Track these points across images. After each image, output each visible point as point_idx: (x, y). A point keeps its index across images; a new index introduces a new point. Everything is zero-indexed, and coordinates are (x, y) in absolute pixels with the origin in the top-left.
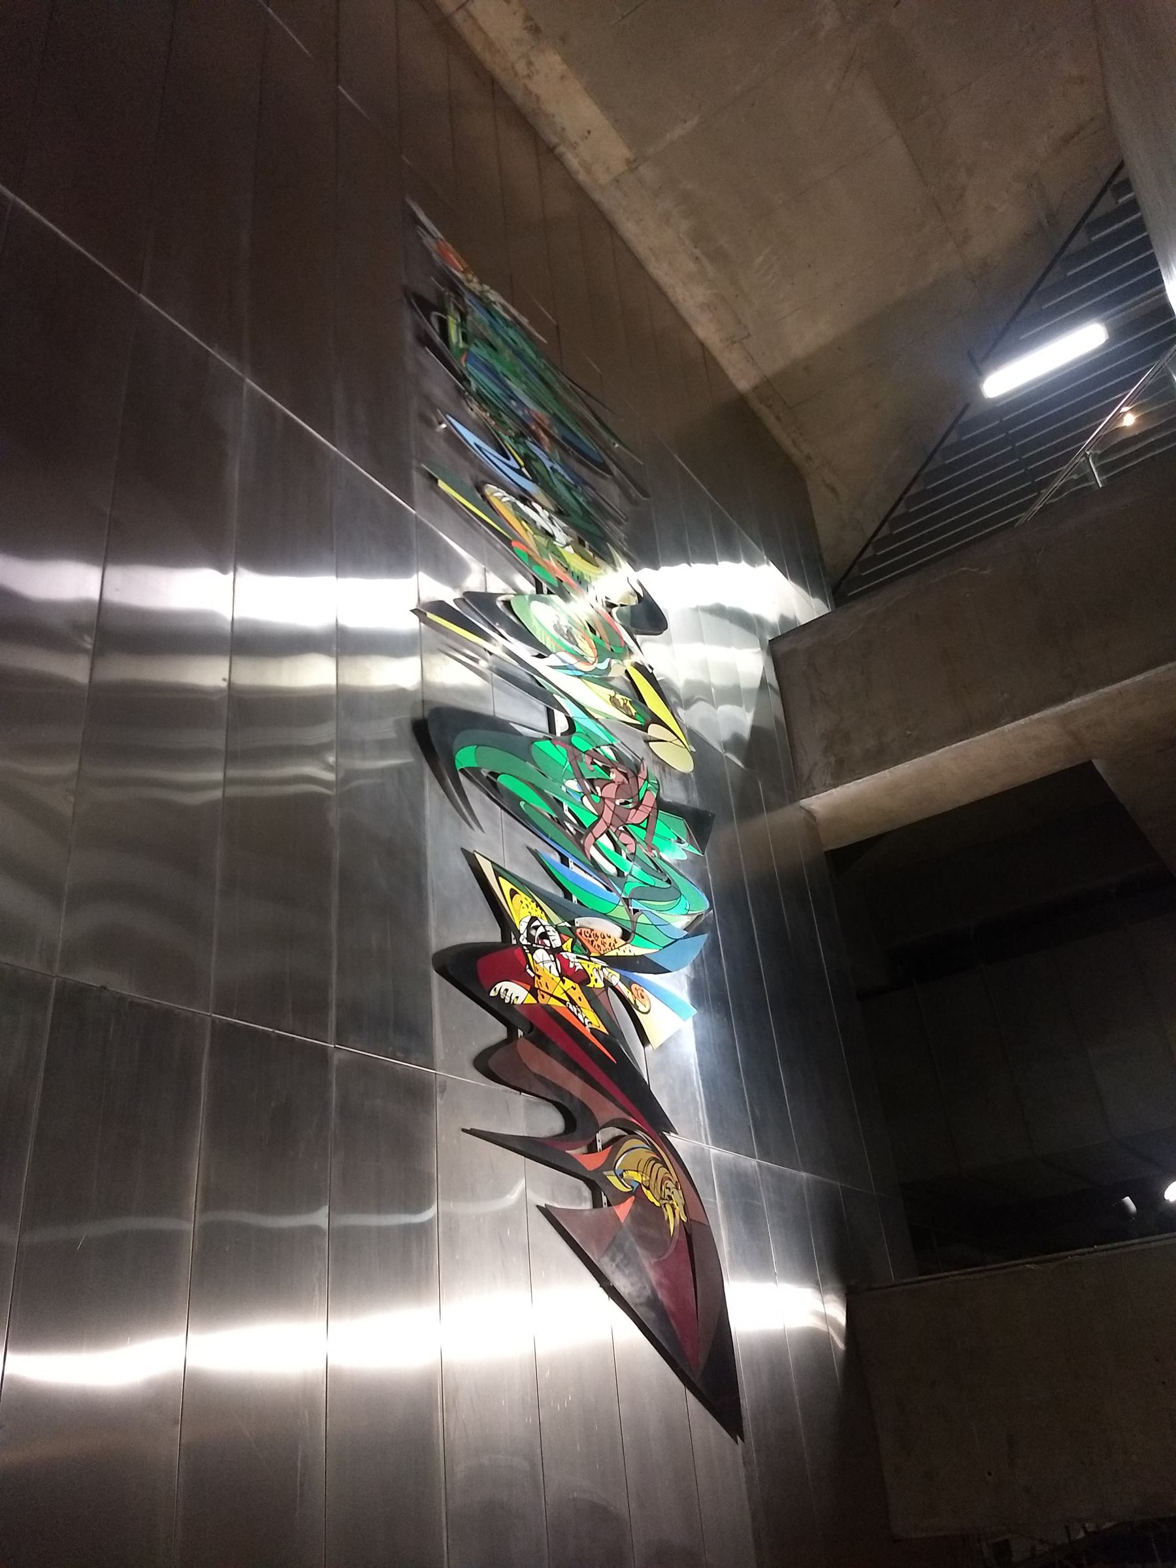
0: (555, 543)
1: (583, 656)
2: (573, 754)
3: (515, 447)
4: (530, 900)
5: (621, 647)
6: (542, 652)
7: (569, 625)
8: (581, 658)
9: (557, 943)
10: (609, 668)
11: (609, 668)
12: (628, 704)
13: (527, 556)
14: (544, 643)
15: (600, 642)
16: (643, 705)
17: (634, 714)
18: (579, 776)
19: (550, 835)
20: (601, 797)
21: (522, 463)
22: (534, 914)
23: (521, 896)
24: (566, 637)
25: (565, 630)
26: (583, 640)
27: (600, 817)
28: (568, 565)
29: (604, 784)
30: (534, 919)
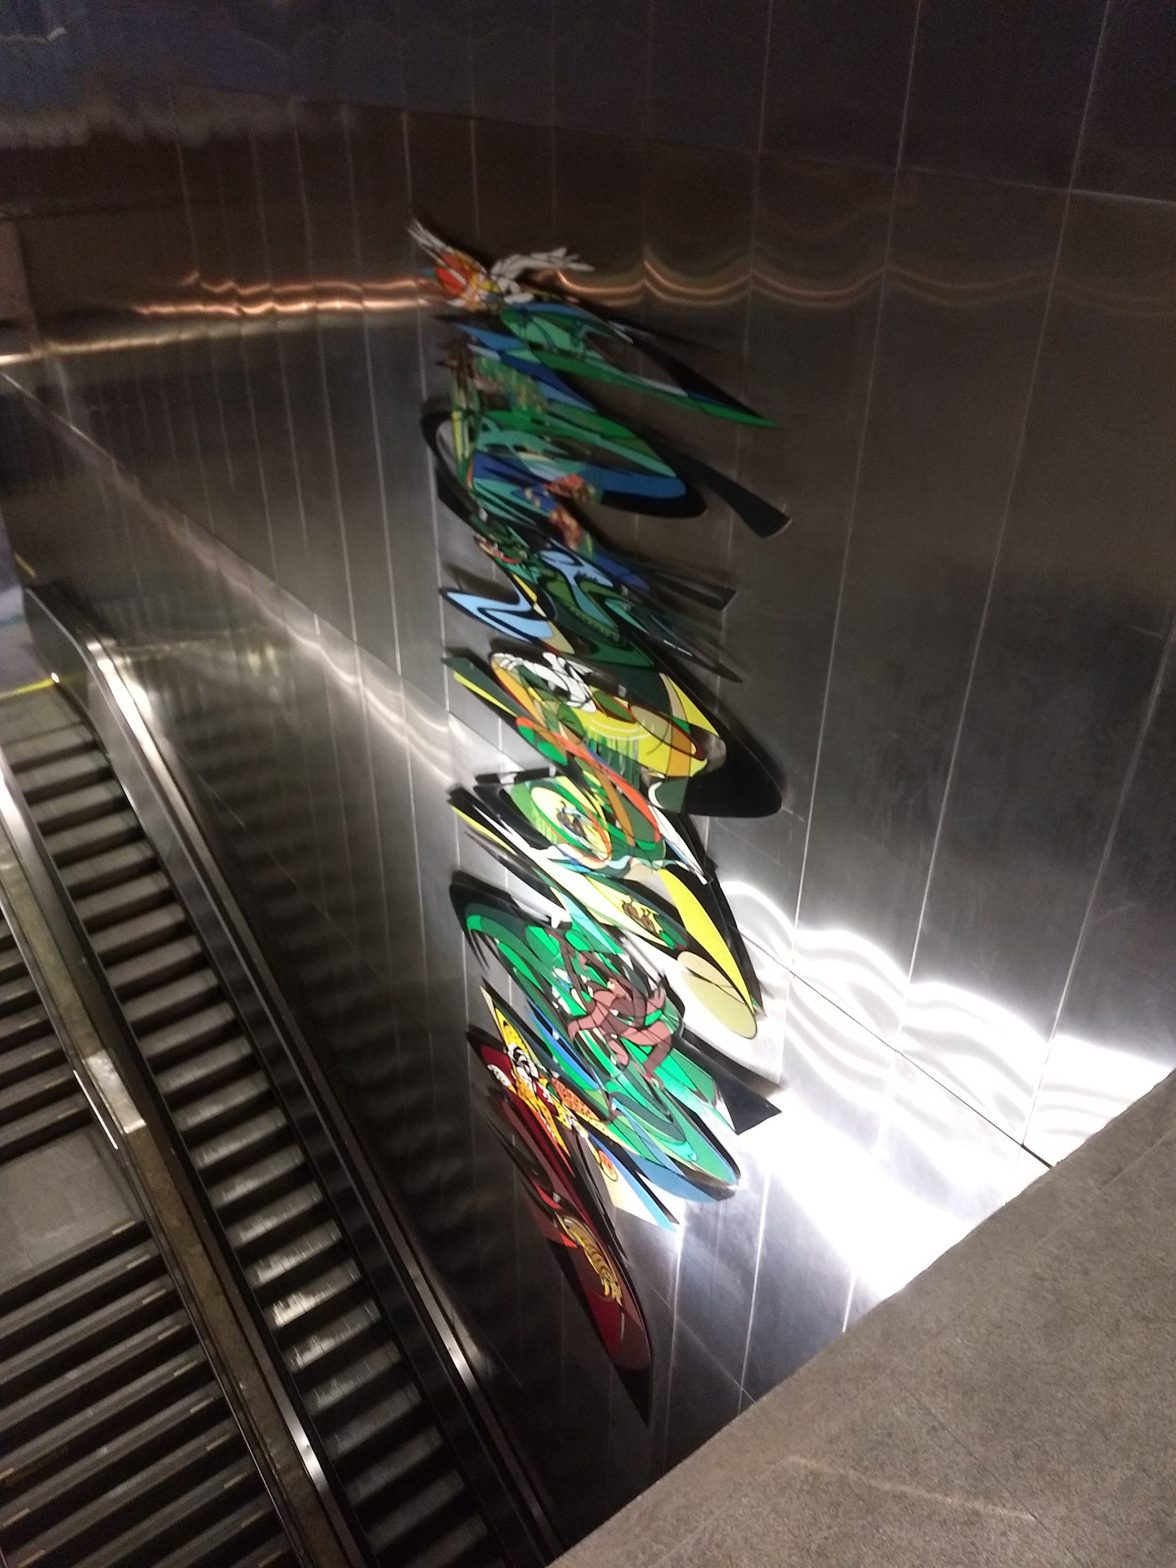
0: (569, 703)
3: (526, 576)
4: (517, 1035)
5: (653, 842)
6: (540, 842)
7: (577, 813)
8: (589, 853)
9: (535, 1074)
10: (628, 868)
11: (628, 868)
12: (651, 918)
13: (532, 733)
14: (543, 834)
16: (680, 927)
17: (658, 932)
18: (571, 971)
20: (593, 999)
21: (534, 597)
24: (571, 827)
25: (571, 819)
26: (594, 831)
27: (589, 1014)
28: (585, 732)
30: (518, 1048)
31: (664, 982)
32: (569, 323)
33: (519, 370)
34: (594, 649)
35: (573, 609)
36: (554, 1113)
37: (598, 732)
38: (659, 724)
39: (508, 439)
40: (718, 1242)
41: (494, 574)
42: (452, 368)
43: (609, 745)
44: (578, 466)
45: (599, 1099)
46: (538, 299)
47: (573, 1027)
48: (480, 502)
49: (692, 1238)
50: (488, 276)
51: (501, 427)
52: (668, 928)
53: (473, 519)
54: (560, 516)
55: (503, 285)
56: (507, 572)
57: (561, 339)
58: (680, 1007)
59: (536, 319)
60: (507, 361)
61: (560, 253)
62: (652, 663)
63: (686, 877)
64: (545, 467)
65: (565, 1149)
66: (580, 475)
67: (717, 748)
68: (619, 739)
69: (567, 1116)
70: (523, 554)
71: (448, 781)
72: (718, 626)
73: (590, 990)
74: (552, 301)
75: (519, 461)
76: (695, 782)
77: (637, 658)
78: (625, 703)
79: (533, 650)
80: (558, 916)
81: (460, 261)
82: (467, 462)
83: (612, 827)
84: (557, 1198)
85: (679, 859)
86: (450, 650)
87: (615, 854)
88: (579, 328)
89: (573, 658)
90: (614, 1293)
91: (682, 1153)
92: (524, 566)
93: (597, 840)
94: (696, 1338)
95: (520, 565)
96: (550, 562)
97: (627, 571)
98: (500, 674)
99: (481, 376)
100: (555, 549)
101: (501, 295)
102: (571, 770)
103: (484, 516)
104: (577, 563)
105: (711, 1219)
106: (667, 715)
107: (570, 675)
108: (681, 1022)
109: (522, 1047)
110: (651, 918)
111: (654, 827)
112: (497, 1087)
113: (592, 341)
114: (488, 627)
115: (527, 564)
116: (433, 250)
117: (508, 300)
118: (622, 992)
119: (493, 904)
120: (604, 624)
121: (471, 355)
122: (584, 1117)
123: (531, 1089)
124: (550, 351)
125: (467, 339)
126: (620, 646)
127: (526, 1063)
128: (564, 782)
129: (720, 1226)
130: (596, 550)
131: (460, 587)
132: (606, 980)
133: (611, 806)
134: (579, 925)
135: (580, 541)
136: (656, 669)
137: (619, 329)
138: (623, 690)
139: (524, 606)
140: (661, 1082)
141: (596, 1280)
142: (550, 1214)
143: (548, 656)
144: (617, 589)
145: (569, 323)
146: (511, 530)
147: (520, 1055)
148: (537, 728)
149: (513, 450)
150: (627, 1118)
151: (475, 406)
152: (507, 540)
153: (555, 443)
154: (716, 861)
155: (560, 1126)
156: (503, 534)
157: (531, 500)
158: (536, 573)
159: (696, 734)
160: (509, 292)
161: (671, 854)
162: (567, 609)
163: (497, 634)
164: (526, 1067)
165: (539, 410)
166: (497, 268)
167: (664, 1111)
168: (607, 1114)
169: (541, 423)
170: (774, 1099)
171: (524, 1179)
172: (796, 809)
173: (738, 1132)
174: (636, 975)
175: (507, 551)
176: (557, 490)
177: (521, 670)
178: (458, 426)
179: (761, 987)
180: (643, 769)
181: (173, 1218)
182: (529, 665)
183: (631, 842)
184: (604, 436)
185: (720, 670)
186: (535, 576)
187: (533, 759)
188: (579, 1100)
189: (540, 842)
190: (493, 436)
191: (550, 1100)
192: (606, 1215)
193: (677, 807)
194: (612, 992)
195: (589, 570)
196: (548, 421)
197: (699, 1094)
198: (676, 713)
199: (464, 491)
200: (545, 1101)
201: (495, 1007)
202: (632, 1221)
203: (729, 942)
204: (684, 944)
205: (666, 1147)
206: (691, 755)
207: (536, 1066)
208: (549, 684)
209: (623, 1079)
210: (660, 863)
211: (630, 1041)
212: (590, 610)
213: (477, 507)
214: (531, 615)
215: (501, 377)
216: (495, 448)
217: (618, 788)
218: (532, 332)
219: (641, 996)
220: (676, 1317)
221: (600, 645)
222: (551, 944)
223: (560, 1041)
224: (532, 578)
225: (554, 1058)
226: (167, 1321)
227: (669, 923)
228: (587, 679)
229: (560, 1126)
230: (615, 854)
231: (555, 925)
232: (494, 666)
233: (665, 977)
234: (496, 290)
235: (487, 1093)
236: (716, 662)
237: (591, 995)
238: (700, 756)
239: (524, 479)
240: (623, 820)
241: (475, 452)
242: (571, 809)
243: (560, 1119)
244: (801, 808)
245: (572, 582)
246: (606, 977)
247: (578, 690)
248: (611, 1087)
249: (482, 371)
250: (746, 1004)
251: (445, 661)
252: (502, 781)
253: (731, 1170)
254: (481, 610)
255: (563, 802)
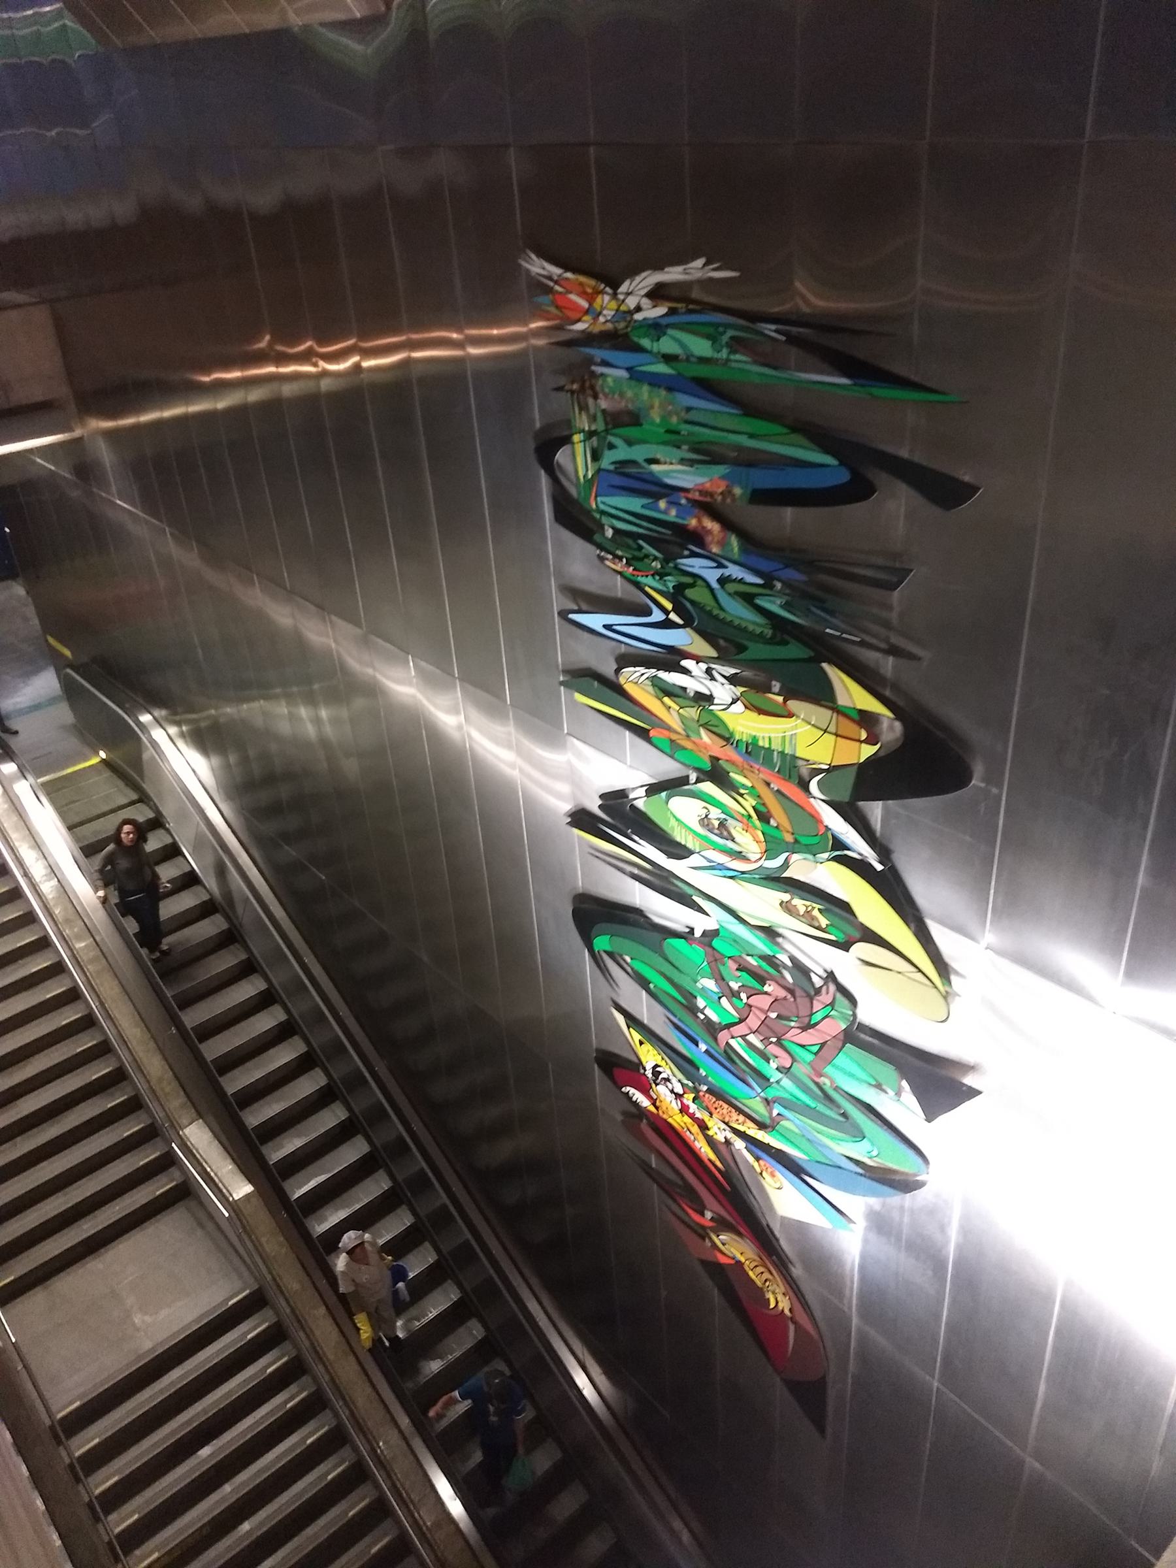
0: (712, 707)
1: (741, 852)
2: (714, 956)
3: (660, 587)
4: (656, 1052)
7: (723, 816)
8: (739, 856)
9: (679, 1090)
11: (786, 865)
12: (816, 913)
13: (669, 742)
14: (683, 843)
15: (775, 833)
16: (852, 918)
17: (824, 926)
18: (720, 979)
19: (678, 1016)
22: (659, 1064)
23: (647, 1047)
24: (716, 831)
25: (716, 823)
27: (741, 1021)
28: (732, 734)
29: (752, 993)
31: (831, 977)
32: (711, 330)
33: (650, 384)
34: (742, 649)
35: (716, 612)
36: (703, 1127)
37: (749, 732)
38: (822, 715)
39: (638, 453)
40: (904, 1237)
41: (619, 588)
42: (572, 392)
43: (761, 743)
44: (721, 470)
45: (757, 1106)
46: (672, 312)
47: (723, 1036)
48: (605, 520)
49: (873, 1237)
50: (614, 295)
51: (630, 443)
52: (837, 921)
53: (597, 537)
54: (699, 521)
55: (631, 302)
56: (639, 586)
57: (701, 347)
58: (853, 1001)
59: (670, 332)
60: (636, 376)
61: (700, 262)
62: (812, 654)
63: (860, 867)
64: (679, 476)
65: (718, 1164)
66: (723, 477)
67: (891, 729)
68: (772, 735)
69: (719, 1129)
70: (657, 565)
71: (566, 807)
72: (890, 608)
73: (743, 996)
74: (690, 312)
75: (651, 473)
76: (865, 769)
77: (794, 650)
78: (780, 699)
79: (671, 659)
80: (701, 924)
81: (581, 284)
82: (589, 482)
83: (764, 824)
84: (709, 1215)
85: (849, 850)
86: (566, 672)
87: (769, 853)
88: (725, 332)
89: (716, 661)
90: (781, 1306)
91: (860, 1151)
92: (657, 578)
93: (749, 842)
94: (882, 1341)
95: (653, 575)
96: (690, 569)
97: (781, 566)
98: (630, 688)
99: (606, 396)
100: (694, 555)
101: (631, 313)
102: (716, 774)
103: (609, 533)
104: (720, 566)
105: (896, 1215)
106: (831, 704)
107: (713, 679)
108: (854, 1015)
109: (663, 1063)
110: (816, 913)
111: (816, 818)
112: (633, 1110)
113: (736, 344)
114: (614, 643)
115: (661, 575)
116: (550, 278)
117: (638, 317)
118: (782, 993)
119: (625, 922)
120: (754, 623)
121: (593, 375)
122: (741, 1128)
123: (675, 1106)
124: (688, 360)
125: (590, 361)
126: (771, 641)
127: (667, 1080)
128: (708, 787)
129: (906, 1220)
130: (743, 550)
131: (578, 606)
132: (763, 985)
133: (764, 804)
134: (726, 929)
135: (723, 543)
136: (818, 659)
137: (769, 329)
138: (776, 686)
139: (657, 616)
140: (832, 1082)
141: (759, 1295)
142: (702, 1233)
143: (685, 663)
144: (768, 585)
145: (711, 330)
146: (641, 542)
147: (660, 1073)
148: (674, 737)
149: (645, 464)
150: (792, 1122)
151: (600, 426)
152: (637, 554)
153: (693, 450)
154: (892, 847)
155: (710, 1141)
156: (629, 547)
157: (665, 510)
158: (671, 582)
159: (866, 719)
160: (638, 309)
161: (838, 844)
162: (710, 613)
163: (623, 649)
164: (668, 1084)
165: (674, 420)
166: (624, 288)
167: (835, 1109)
168: (768, 1121)
169: (678, 433)
170: (969, 1080)
171: (670, 1202)
172: (987, 779)
173: (929, 1120)
174: (799, 974)
175: (639, 565)
176: (697, 496)
177: (655, 681)
178: (579, 448)
179: (950, 970)
180: (800, 763)
181: (293, 1280)
182: (663, 675)
183: (789, 838)
184: (752, 436)
185: (893, 651)
186: (671, 585)
187: (669, 768)
188: (734, 1110)
189: (679, 851)
190: (622, 452)
191: (698, 1115)
192: (768, 1225)
193: (844, 796)
194: (770, 995)
195: (734, 571)
196: (685, 429)
197: (879, 1086)
198: (842, 700)
199: (588, 512)
200: (692, 1116)
201: (629, 1028)
202: (799, 1229)
203: (912, 925)
204: (856, 934)
205: (843, 1147)
206: (861, 742)
207: (679, 1081)
208: (688, 691)
209: (786, 1082)
210: (826, 855)
211: (793, 1042)
212: (737, 611)
213: (601, 527)
214: (667, 624)
215: (630, 394)
216: (622, 465)
217: (772, 786)
218: (667, 345)
219: (804, 995)
220: (855, 1321)
221: (746, 643)
222: (695, 954)
223: (707, 1052)
224: (668, 588)
225: (701, 1071)
226: (293, 1388)
227: (836, 915)
228: (732, 680)
229: (710, 1141)
230: (769, 853)
231: (698, 933)
232: (622, 680)
233: (832, 972)
234: (623, 308)
235: (619, 1118)
236: (887, 640)
237: (745, 1000)
238: (871, 741)
239: (658, 489)
240: (779, 816)
241: (599, 471)
242: (715, 813)
243: (710, 1133)
244: (993, 778)
245: (715, 585)
246: (762, 980)
247: (722, 692)
248: (771, 1093)
249: (607, 390)
250: (936, 987)
251: (562, 683)
252: (631, 796)
253: (919, 1160)
254: (608, 627)
255: (706, 808)
